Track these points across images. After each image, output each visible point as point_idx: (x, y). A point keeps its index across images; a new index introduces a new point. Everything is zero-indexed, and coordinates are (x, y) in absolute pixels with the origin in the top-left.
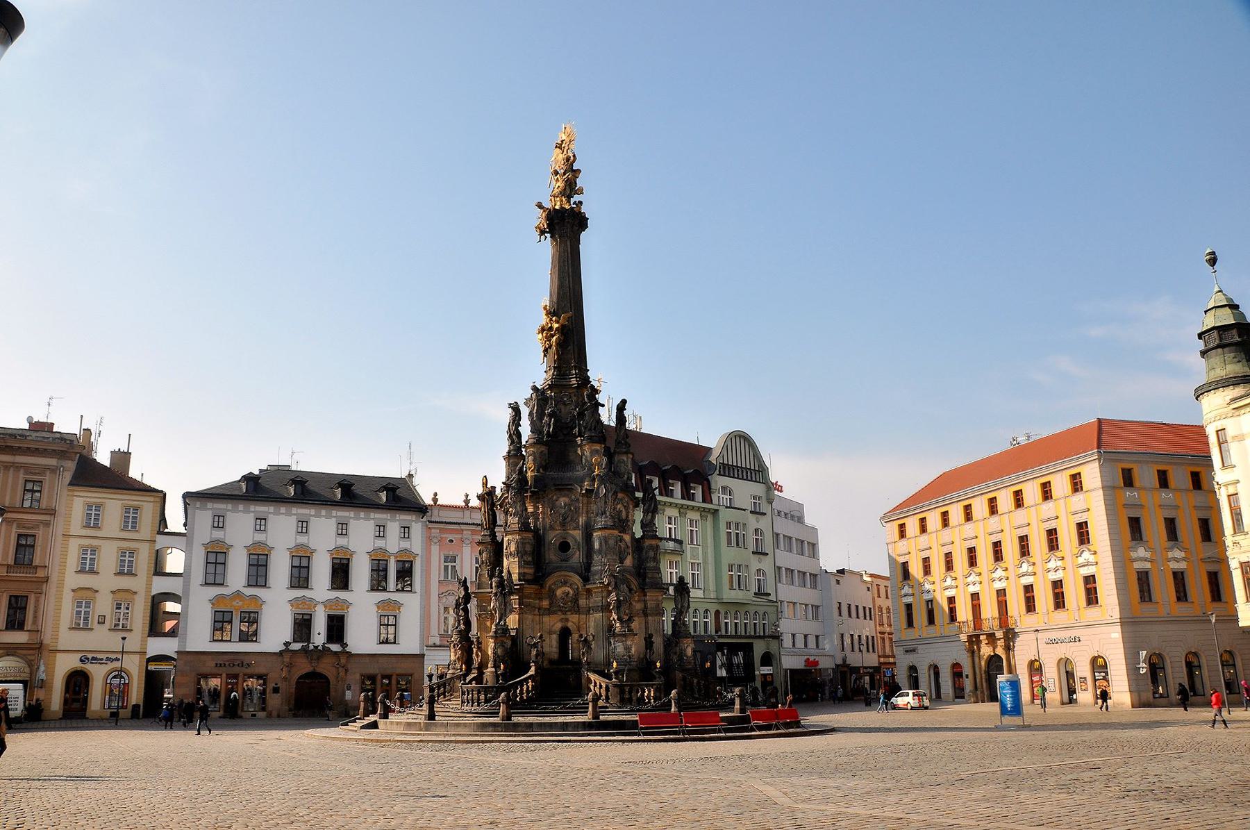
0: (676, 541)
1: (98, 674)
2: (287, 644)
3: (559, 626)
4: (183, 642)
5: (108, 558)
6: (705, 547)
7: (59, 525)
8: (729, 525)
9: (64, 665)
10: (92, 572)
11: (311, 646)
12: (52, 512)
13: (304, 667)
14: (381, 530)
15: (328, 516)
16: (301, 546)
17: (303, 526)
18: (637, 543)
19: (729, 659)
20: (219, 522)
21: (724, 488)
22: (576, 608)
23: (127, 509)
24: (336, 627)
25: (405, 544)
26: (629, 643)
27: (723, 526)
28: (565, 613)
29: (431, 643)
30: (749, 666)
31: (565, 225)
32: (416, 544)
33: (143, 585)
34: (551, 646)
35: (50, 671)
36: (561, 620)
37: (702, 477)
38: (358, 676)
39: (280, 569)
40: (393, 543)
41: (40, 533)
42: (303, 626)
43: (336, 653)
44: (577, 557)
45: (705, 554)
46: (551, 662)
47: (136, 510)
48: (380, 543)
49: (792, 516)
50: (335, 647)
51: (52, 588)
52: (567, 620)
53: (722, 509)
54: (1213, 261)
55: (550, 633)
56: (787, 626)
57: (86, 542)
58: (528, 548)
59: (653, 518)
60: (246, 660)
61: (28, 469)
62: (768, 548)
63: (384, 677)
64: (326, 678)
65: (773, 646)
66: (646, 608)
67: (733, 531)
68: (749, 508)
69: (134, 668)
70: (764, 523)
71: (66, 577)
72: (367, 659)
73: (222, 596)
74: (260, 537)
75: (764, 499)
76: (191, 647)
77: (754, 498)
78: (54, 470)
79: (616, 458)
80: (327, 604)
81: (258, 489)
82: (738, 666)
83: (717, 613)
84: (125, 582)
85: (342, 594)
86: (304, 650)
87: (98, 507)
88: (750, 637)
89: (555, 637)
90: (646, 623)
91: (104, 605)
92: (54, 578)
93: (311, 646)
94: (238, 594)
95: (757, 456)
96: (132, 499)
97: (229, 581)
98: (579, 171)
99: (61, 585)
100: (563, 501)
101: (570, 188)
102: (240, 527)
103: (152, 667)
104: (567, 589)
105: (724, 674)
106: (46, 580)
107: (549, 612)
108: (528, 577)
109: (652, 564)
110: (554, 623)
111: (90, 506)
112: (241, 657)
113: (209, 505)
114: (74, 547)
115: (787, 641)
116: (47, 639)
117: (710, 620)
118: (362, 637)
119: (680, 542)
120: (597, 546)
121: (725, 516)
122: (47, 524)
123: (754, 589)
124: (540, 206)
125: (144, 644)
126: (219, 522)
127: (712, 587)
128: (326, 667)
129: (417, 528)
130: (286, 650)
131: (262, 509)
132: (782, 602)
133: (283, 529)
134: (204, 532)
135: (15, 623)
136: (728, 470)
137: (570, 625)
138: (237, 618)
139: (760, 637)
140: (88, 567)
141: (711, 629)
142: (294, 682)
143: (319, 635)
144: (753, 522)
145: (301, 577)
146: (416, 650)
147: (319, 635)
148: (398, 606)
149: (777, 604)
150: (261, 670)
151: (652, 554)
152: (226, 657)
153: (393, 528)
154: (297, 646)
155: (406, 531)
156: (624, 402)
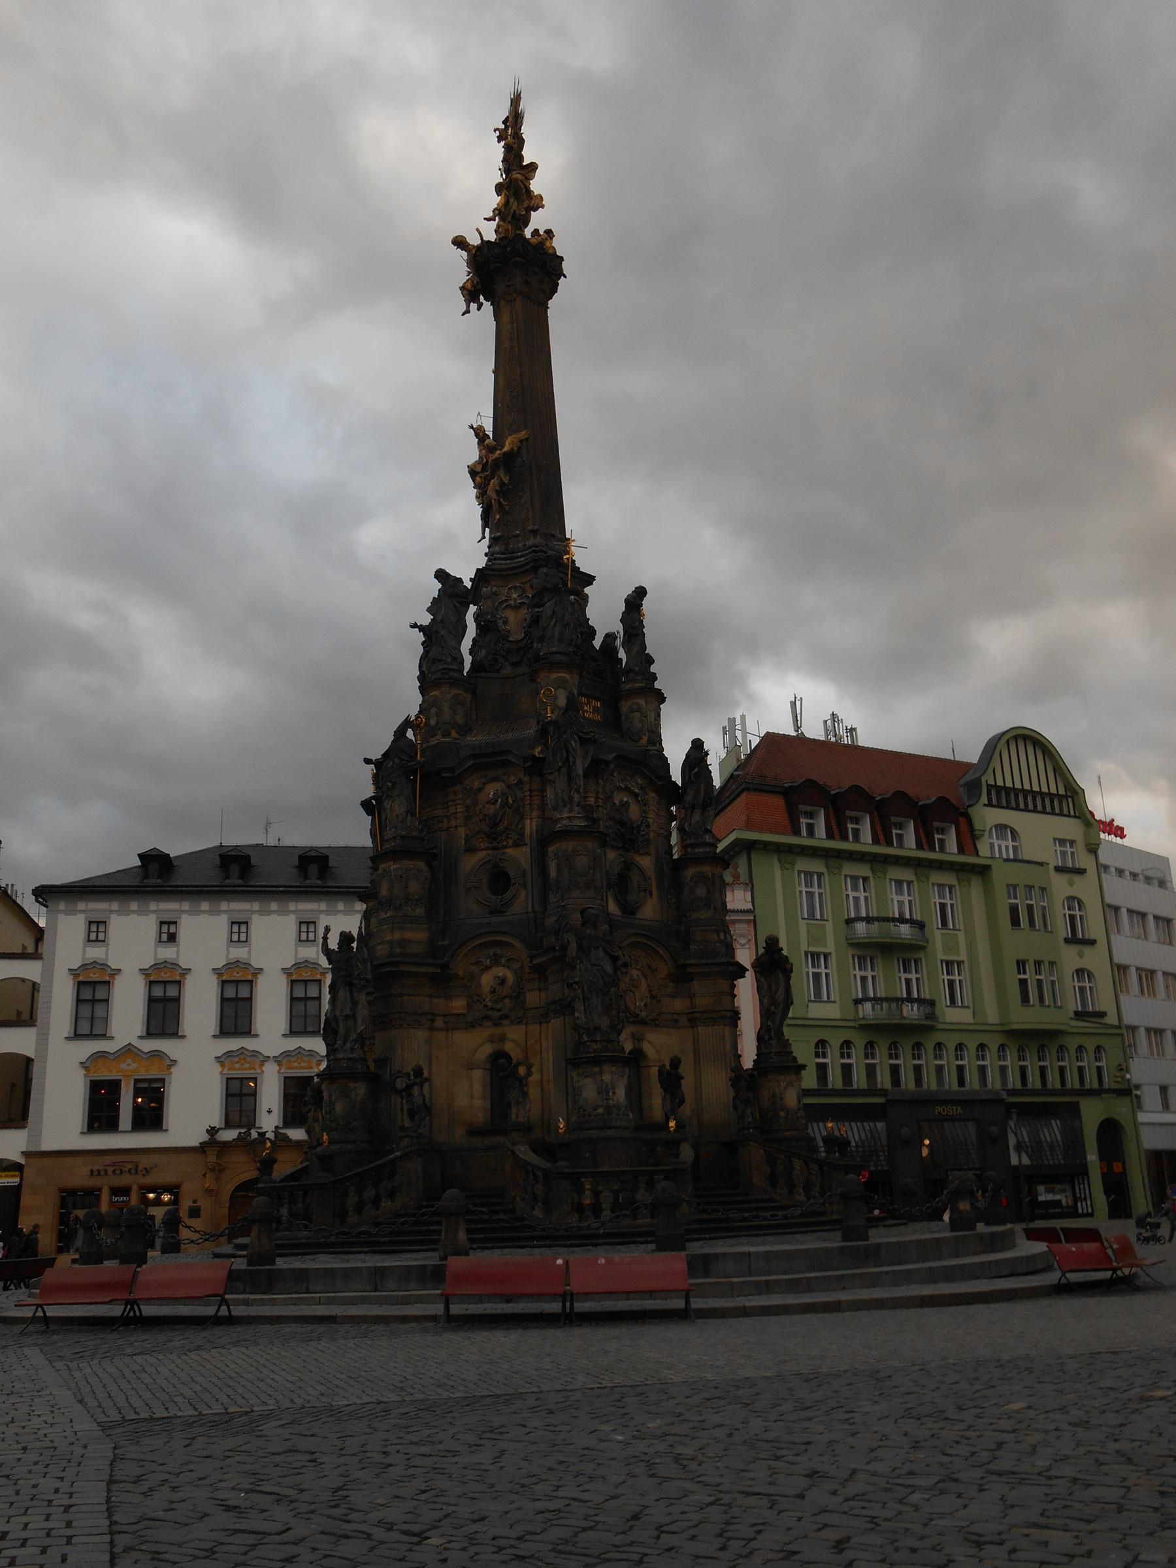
0: (911, 922)
2: (212, 1131)
3: (488, 1049)
4: (36, 1136)
13: (243, 1170)
15: (282, 912)
16: (236, 964)
20: (96, 930)
21: (1001, 828)
26: (607, 1077)
28: (497, 1024)
36: (491, 1041)
39: (200, 1006)
42: (239, 1097)
43: (299, 1144)
45: (971, 945)
46: (474, 1132)
52: (503, 1039)
55: (471, 1067)
56: (1144, 1070)
60: (145, 1161)
62: (1094, 927)
65: (1120, 1109)
67: (1020, 902)
70: (1083, 888)
76: (50, 1142)
77: (1062, 842)
79: (625, 707)
80: (282, 1059)
81: (156, 877)
86: (242, 1143)
88: (1073, 1092)
89: (477, 1074)
93: (254, 1134)
94: (129, 1051)
98: (533, 167)
100: (491, 790)
102: (132, 940)
104: (500, 971)
105: (1026, 1161)
110: (475, 1044)
112: (136, 1158)
113: (81, 906)
115: (1150, 1097)
119: (920, 925)
120: (553, 872)
121: (1001, 876)
123: (1073, 1004)
124: (460, 242)
126: (96, 930)
130: (211, 1145)
131: (168, 907)
132: (1133, 1029)
133: (205, 939)
136: (1007, 797)
137: (509, 1047)
139: (1091, 1093)
142: (226, 1197)
144: (1061, 887)
145: (236, 1015)
149: (1124, 1033)
150: (169, 1178)
151: (701, 891)
152: (107, 1159)
154: (230, 1135)
156: (641, 592)
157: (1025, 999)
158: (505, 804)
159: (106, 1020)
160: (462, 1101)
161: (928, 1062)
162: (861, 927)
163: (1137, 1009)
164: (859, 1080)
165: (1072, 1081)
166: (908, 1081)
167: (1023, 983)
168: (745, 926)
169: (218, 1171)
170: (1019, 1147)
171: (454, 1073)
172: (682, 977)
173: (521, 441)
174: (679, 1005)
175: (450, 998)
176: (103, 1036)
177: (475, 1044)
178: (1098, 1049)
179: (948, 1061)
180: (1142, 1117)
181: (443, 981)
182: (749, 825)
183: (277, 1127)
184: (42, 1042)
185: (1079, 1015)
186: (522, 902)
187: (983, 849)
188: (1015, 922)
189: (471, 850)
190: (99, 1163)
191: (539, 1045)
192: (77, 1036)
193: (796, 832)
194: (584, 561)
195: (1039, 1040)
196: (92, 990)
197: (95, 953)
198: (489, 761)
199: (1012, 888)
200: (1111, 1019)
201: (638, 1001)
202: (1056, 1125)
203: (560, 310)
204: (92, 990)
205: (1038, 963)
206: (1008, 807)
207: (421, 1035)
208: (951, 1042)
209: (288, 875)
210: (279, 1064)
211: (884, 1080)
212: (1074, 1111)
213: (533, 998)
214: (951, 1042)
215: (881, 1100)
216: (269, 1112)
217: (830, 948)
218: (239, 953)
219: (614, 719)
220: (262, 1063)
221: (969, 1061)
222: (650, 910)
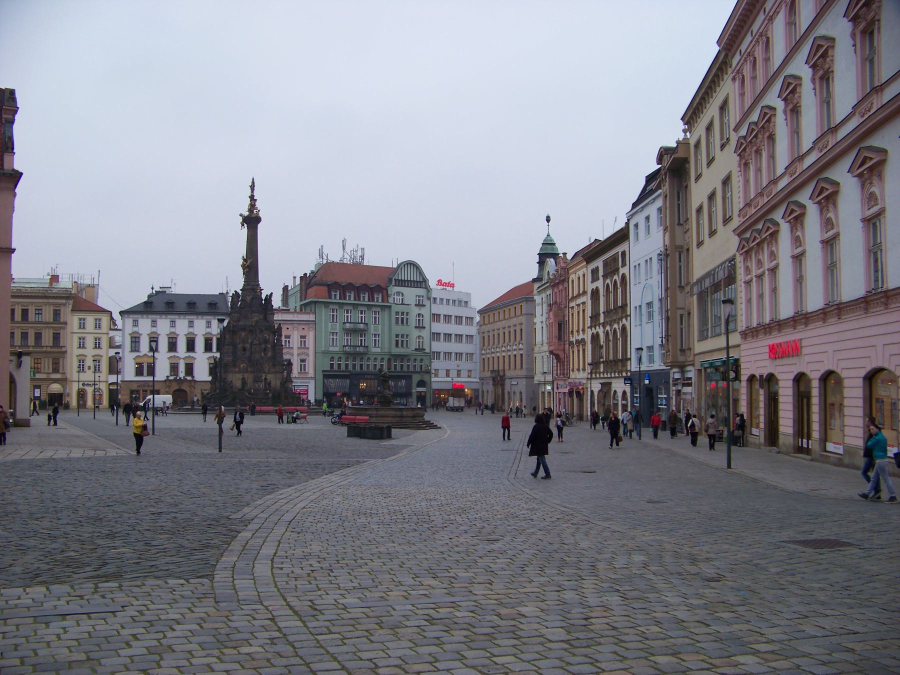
1: (90, 390)
4: (123, 377)
5: (90, 342)
6: (383, 325)
7: (69, 327)
8: (397, 313)
9: (75, 387)
10: (84, 347)
12: (66, 323)
17: (173, 323)
20: (136, 323)
21: (398, 293)
23: (96, 320)
24: (190, 369)
27: (393, 314)
30: (409, 386)
31: (252, 221)
33: (107, 353)
34: (238, 384)
35: (71, 389)
37: (382, 290)
39: (163, 344)
41: (62, 332)
44: (248, 354)
45: (383, 330)
47: (100, 320)
48: (209, 330)
49: (460, 302)
50: (189, 378)
51: (68, 355)
53: (393, 305)
54: (548, 219)
57: (80, 335)
61: (54, 304)
65: (426, 378)
67: (400, 316)
68: (413, 303)
69: (104, 387)
70: (424, 311)
71: (74, 352)
73: (138, 356)
74: (154, 329)
75: (425, 298)
78: (64, 305)
83: (389, 360)
84: (97, 352)
85: (191, 354)
87: (84, 319)
91: (89, 362)
92: (69, 351)
94: (145, 355)
95: (421, 273)
96: (98, 316)
97: (141, 350)
99: (72, 355)
101: (252, 206)
102: (145, 326)
103: (111, 387)
106: (66, 352)
107: (239, 372)
110: (240, 376)
111: (80, 319)
114: (76, 338)
115: (442, 373)
116: (68, 377)
117: (385, 363)
119: (367, 324)
121: (395, 309)
122: (64, 328)
124: (241, 215)
125: (107, 378)
126: (136, 323)
127: (386, 345)
128: (185, 387)
130: (167, 380)
131: (154, 317)
133: (163, 326)
134: (129, 328)
135: (56, 370)
138: (146, 368)
139: (417, 372)
140: (82, 346)
141: (385, 369)
143: (182, 374)
144: (416, 311)
145: (172, 347)
147: (182, 374)
154: (172, 378)
157: (397, 345)
159: (139, 347)
161: (365, 363)
163: (437, 346)
164: (343, 368)
165: (412, 369)
166: (358, 368)
167: (397, 341)
169: (169, 387)
171: (235, 379)
172: (274, 365)
176: (138, 351)
177: (240, 376)
178: (422, 360)
179: (371, 363)
180: (433, 379)
181: (235, 366)
182: (315, 296)
184: (123, 352)
185: (416, 350)
186: (248, 354)
187: (391, 300)
188: (397, 323)
190: (139, 384)
191: (249, 377)
192: (132, 351)
193: (330, 298)
194: (262, 286)
195: (402, 357)
196: (135, 341)
197: (135, 329)
198: (244, 329)
199: (397, 313)
200: (427, 351)
201: (266, 370)
202: (404, 382)
203: (260, 226)
204: (135, 341)
205: (403, 336)
208: (372, 358)
209: (183, 307)
211: (350, 368)
212: (410, 377)
213: (249, 369)
214: (372, 358)
217: (337, 331)
218: (173, 330)
219: (265, 318)
221: (378, 363)
222: (269, 354)
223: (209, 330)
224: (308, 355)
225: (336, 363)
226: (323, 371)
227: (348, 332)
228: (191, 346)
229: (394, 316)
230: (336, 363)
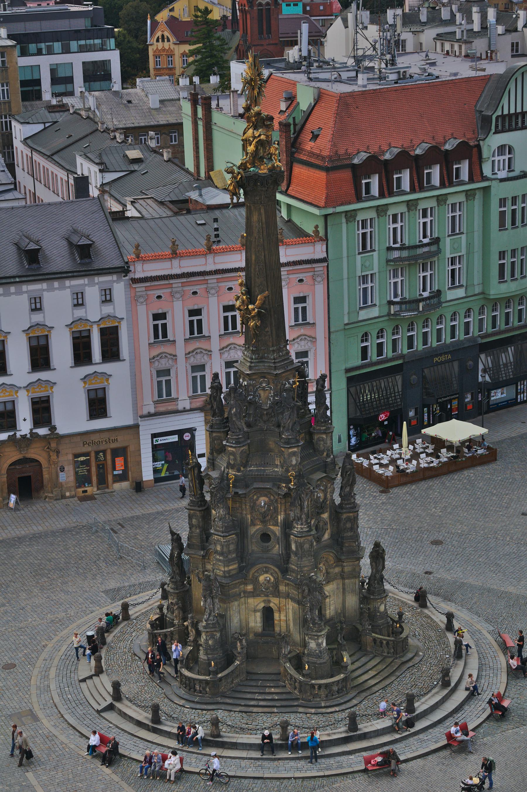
3: (262, 605)
11: (18, 434)
14: (79, 302)
18: (336, 512)
19: (496, 362)
22: (277, 593)
24: (42, 410)
25: (108, 309)
26: (320, 641)
27: (495, 209)
28: (267, 596)
29: (145, 412)
32: (119, 307)
34: (256, 622)
36: (264, 601)
38: (70, 457)
40: (94, 311)
43: (45, 436)
44: (277, 549)
46: (256, 635)
48: (80, 313)
50: (43, 431)
52: (269, 601)
53: (494, 184)
55: (255, 611)
58: (232, 547)
59: (352, 489)
63: (97, 453)
64: (37, 461)
66: (343, 571)
72: (78, 439)
79: (316, 437)
80: (28, 387)
82: (505, 365)
85: (43, 375)
86: (12, 439)
89: (259, 615)
90: (344, 584)
100: (262, 501)
104: (268, 576)
107: (254, 594)
108: (233, 572)
109: (349, 534)
110: (258, 603)
118: (71, 417)
121: (499, 191)
128: (35, 452)
129: (119, 288)
137: (272, 605)
146: (130, 422)
148: (107, 376)
151: (349, 525)
153: (93, 294)
155: (107, 298)
158: (269, 509)
160: (252, 624)
162: (396, 254)
168: (321, 269)
170: (485, 371)
172: (339, 561)
173: (265, 297)
174: (337, 570)
175: (246, 584)
177: (258, 603)
179: (445, 326)
183: (31, 430)
189: (253, 524)
202: (511, 350)
205: (514, 252)
206: (510, 130)
207: (236, 603)
210: (28, 391)
215: (400, 362)
216: (25, 420)
220: (17, 392)
223: (80, 313)
224: (313, 339)
225: (372, 344)
226: (347, 371)
227: (396, 266)
228: (40, 358)
229: (495, 209)
230: (372, 344)
